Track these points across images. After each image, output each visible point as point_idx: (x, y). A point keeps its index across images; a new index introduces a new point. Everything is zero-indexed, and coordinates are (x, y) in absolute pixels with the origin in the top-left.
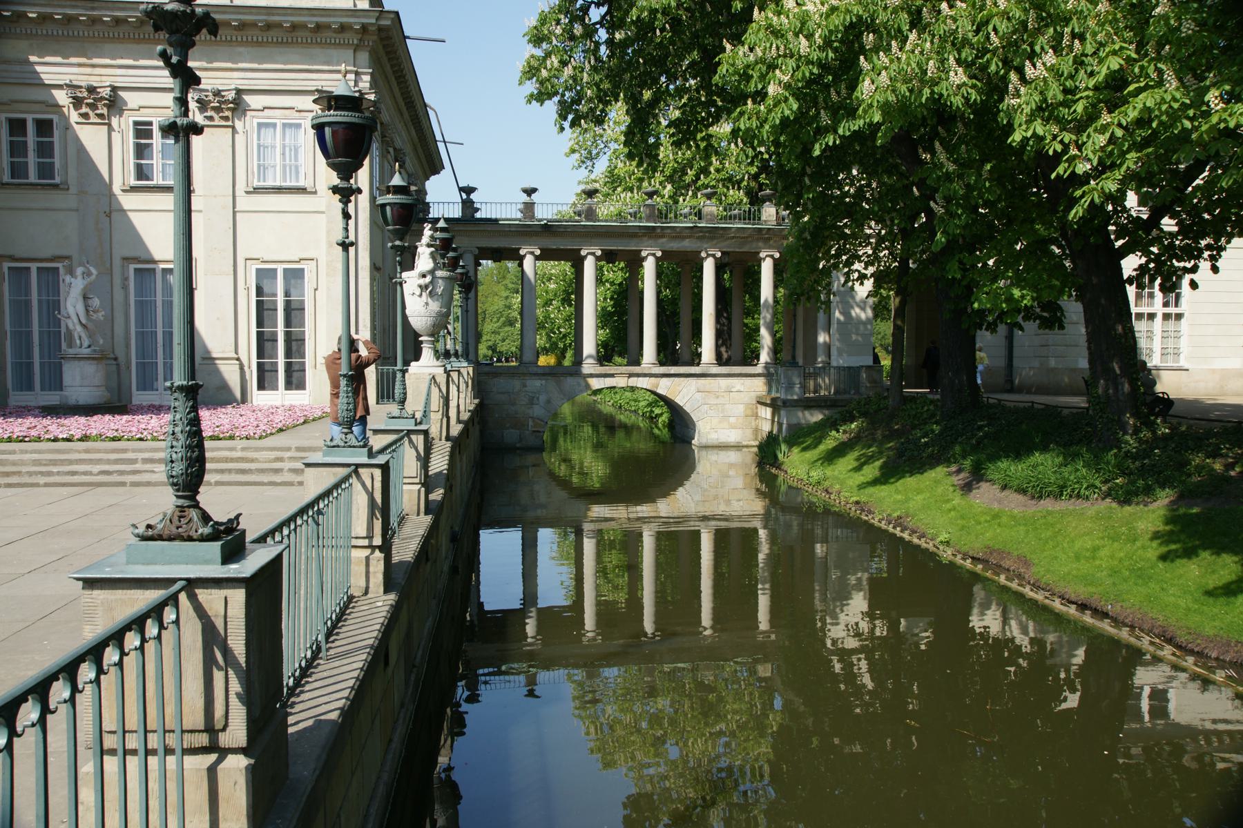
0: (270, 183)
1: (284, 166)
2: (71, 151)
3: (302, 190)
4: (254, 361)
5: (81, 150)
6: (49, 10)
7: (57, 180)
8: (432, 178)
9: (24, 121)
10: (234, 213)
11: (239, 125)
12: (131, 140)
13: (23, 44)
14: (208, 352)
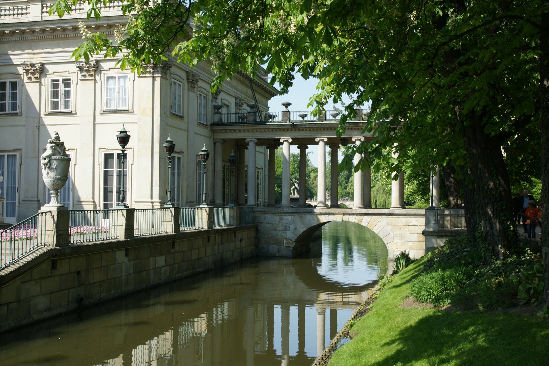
0: (113, 108)
1: (119, 99)
2: (24, 97)
3: (127, 111)
4: (102, 203)
5: (28, 95)
6: (66, 25)
7: (18, 111)
8: (272, 98)
9: (5, 83)
10: (94, 125)
11: (98, 78)
12: (50, 89)
13: (6, 46)
14: (79, 198)
